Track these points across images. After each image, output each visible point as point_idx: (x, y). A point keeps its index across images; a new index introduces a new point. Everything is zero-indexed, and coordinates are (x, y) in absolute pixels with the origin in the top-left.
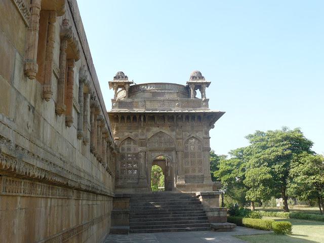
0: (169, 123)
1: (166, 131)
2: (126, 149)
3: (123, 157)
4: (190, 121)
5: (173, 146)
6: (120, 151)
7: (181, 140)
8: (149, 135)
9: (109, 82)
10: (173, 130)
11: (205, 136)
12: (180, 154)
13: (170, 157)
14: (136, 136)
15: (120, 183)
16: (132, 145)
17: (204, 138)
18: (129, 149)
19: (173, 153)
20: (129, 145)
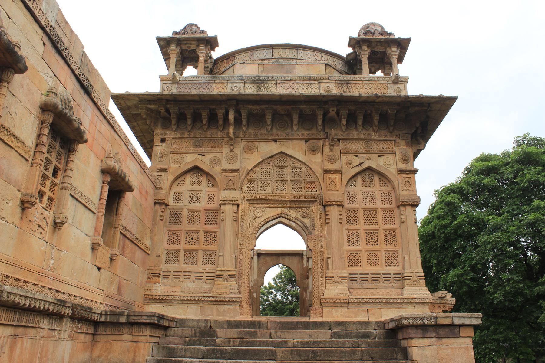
0: (305, 133)
1: (296, 150)
2: (187, 195)
3: (176, 217)
4: (360, 128)
5: (315, 192)
6: (171, 203)
7: (337, 176)
8: (250, 161)
9: (159, 40)
10: (314, 150)
11: (402, 166)
12: (334, 212)
13: (307, 221)
14: (215, 163)
15: (160, 288)
16: (204, 187)
17: (401, 171)
18: (194, 197)
19: (315, 209)
20: (197, 188)
